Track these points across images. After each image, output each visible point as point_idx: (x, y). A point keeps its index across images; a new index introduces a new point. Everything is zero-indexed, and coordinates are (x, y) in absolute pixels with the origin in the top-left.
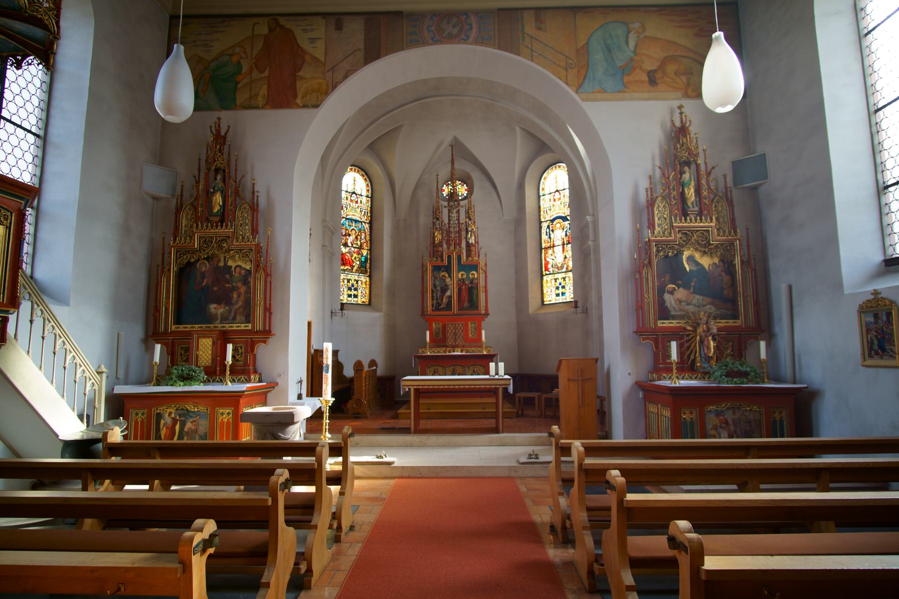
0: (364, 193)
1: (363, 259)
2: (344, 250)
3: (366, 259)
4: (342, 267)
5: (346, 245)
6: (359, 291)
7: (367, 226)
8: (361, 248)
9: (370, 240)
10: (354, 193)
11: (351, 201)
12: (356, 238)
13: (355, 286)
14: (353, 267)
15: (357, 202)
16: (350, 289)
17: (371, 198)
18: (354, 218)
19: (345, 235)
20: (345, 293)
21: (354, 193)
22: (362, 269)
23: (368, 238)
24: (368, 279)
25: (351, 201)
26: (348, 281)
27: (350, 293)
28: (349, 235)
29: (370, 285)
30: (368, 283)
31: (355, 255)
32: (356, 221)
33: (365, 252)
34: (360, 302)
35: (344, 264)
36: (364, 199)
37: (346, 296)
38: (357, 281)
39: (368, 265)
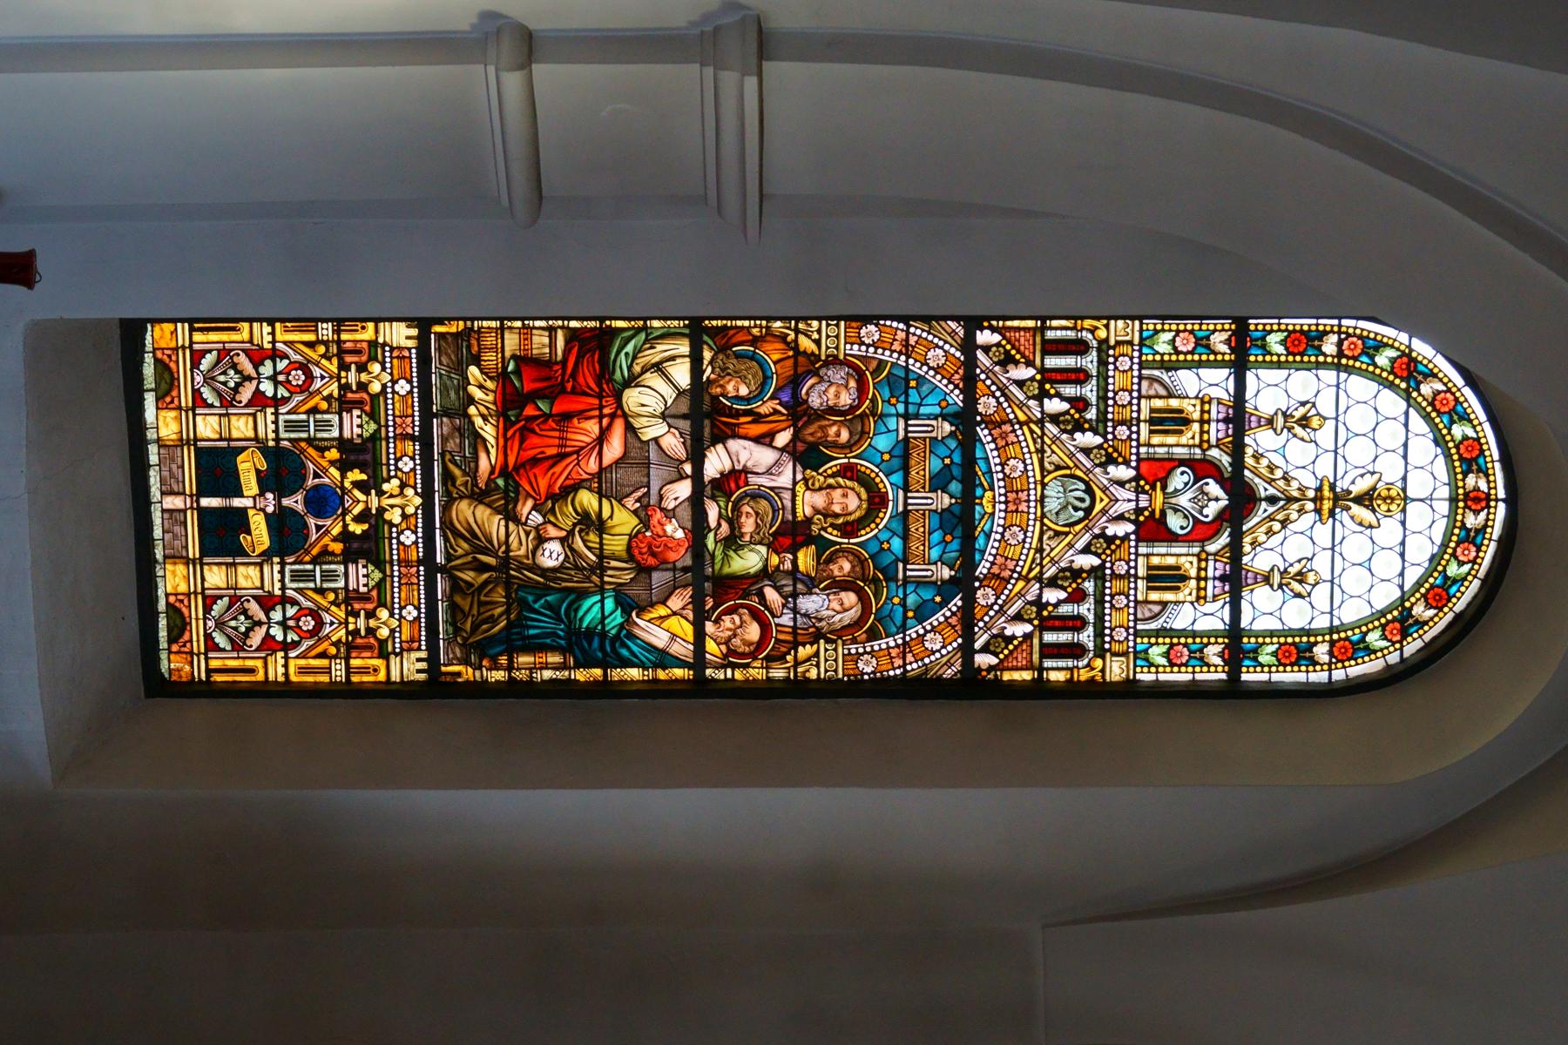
0: (1264, 609)
1: (591, 611)
2: (648, 400)
3: (607, 648)
4: (480, 388)
5: (706, 417)
6: (272, 577)
7: (936, 648)
8: (715, 591)
9: (798, 688)
10: (1242, 500)
11: (1153, 473)
12: (792, 534)
13: (326, 532)
14: (502, 495)
15: (1152, 529)
16: (282, 470)
17: (1233, 690)
18: (990, 503)
19: (799, 413)
20: (241, 427)
21: (1242, 500)
22: (496, 606)
23: (821, 663)
24: (410, 667)
25: (1153, 473)
26: (358, 454)
27: (248, 467)
28: (807, 455)
29: (347, 691)
30: (372, 669)
31: (623, 521)
32: (961, 523)
33: (666, 629)
34: (173, 580)
35: (510, 404)
36: (1201, 615)
37: (207, 427)
38: (367, 546)
39: (548, 668)
